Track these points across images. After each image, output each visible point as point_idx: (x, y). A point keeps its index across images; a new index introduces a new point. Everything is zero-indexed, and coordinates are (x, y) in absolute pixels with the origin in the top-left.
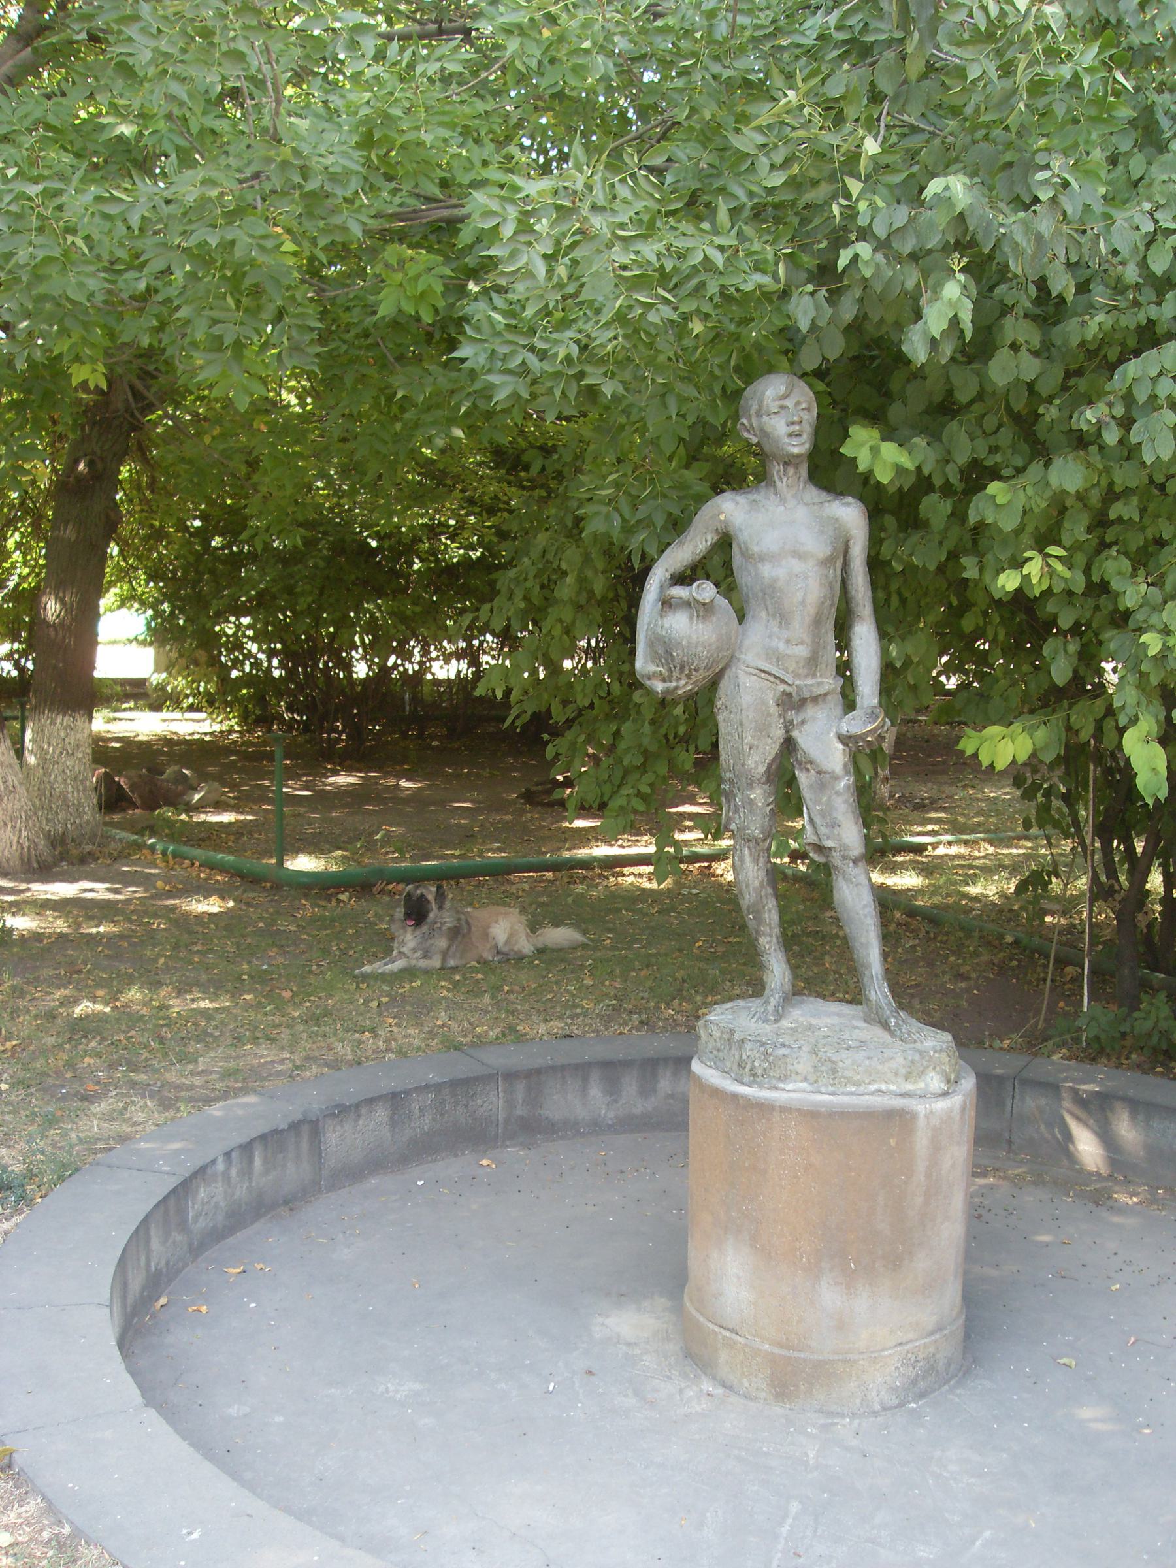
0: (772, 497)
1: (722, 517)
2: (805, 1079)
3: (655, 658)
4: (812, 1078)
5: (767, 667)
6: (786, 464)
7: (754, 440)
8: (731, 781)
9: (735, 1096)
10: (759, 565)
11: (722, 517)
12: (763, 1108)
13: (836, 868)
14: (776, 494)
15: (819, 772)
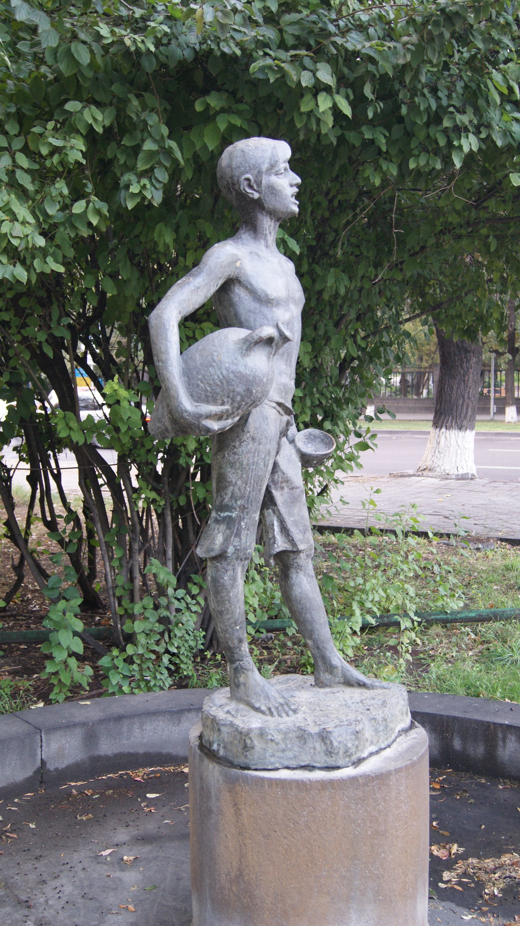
0: (263, 248)
1: (238, 264)
2: (372, 743)
3: (197, 397)
4: (375, 741)
5: (281, 401)
6: (278, 220)
7: (256, 196)
8: (243, 508)
9: (354, 779)
10: (275, 309)
11: (238, 264)
12: (380, 778)
13: (299, 567)
14: (267, 247)
15: (292, 489)
